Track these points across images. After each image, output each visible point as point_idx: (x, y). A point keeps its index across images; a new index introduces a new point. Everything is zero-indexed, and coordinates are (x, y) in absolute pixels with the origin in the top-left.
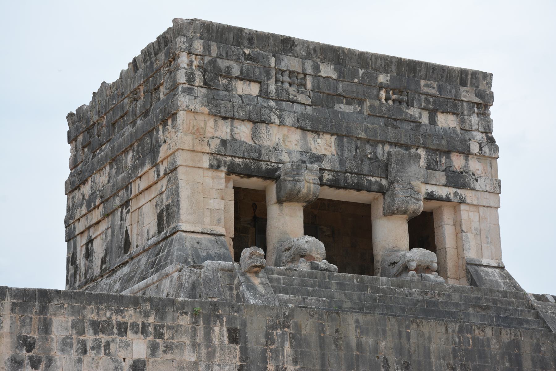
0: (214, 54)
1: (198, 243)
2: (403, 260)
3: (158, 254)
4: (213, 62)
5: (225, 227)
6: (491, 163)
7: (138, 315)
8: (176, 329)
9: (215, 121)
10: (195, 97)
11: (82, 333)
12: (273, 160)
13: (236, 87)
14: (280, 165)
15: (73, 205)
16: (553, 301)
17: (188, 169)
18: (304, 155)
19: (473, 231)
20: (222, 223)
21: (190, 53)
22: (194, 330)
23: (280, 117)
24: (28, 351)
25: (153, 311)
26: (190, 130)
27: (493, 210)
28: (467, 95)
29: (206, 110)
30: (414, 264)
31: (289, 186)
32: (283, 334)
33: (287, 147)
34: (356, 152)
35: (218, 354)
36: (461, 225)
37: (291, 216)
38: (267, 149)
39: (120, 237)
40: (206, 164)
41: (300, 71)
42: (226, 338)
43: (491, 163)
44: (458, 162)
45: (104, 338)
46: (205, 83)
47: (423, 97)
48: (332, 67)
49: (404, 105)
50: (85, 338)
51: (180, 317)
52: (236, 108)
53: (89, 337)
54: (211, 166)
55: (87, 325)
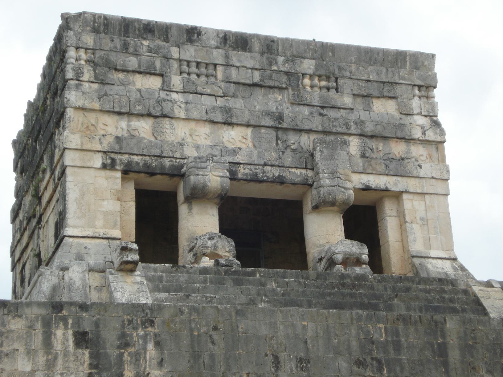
5: (122, 228)
6: (437, 148)
8: (6, 335)
12: (178, 156)
13: (133, 81)
16: (499, 286)
17: (76, 169)
18: (215, 150)
19: (419, 221)
20: (119, 226)
21: (77, 48)
26: (79, 128)
27: (442, 198)
30: (340, 257)
32: (146, 335)
33: (195, 142)
34: (277, 144)
36: (404, 216)
38: (170, 144)
40: (98, 164)
42: (71, 343)
43: (437, 148)
49: (333, 92)
51: (13, 321)
52: (132, 103)
54: (104, 166)
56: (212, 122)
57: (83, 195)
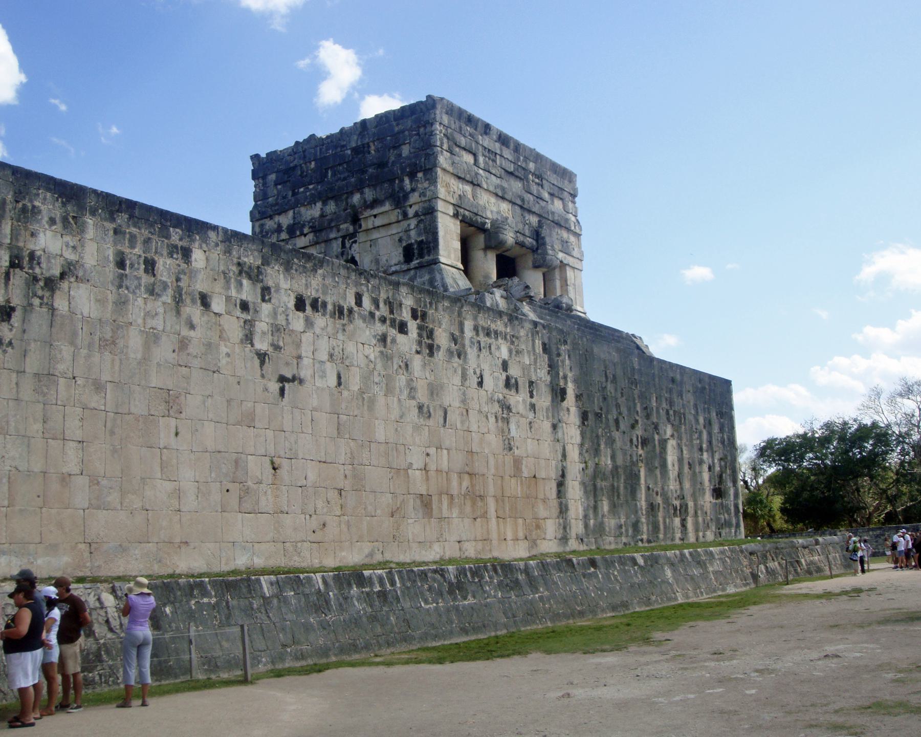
11: (477, 334)
15: (261, 232)
36: (566, 281)
45: (489, 340)
55: (480, 329)
56: (497, 195)
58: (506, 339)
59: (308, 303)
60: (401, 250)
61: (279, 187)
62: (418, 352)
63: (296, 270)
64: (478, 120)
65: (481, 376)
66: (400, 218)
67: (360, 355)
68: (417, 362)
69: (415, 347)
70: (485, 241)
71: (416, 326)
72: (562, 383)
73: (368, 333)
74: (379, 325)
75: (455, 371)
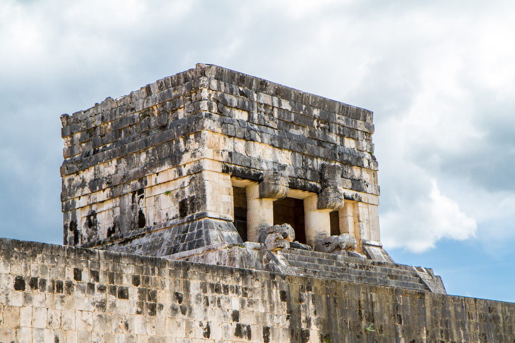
0: (223, 91)
1: (220, 226)
2: (336, 241)
3: (186, 231)
4: (222, 96)
7: (234, 281)
9: (225, 139)
10: (214, 121)
11: (205, 291)
14: (262, 172)
15: (70, 186)
17: (210, 172)
21: (209, 89)
22: (263, 291)
23: (261, 137)
24: (180, 302)
25: (241, 278)
28: (360, 125)
29: (219, 130)
30: (344, 245)
31: (273, 187)
32: (309, 295)
35: (275, 308)
36: (358, 217)
37: (267, 208)
39: (133, 215)
41: (271, 104)
42: (279, 298)
44: (356, 172)
45: (217, 295)
46: (218, 111)
47: (337, 126)
48: (288, 102)
50: (207, 295)
52: (236, 130)
53: (210, 294)
54: (223, 171)
55: (208, 286)
57: (214, 190)
58: (237, 292)
59: (27, 283)
60: (177, 205)
61: (84, 145)
62: (138, 313)
63: (16, 258)
64: (252, 79)
65: (208, 328)
66: (177, 176)
67: (78, 320)
68: (137, 322)
69: (135, 308)
70: (260, 191)
71: (137, 290)
72: (304, 326)
73: (86, 301)
74: (99, 293)
75: (179, 326)
